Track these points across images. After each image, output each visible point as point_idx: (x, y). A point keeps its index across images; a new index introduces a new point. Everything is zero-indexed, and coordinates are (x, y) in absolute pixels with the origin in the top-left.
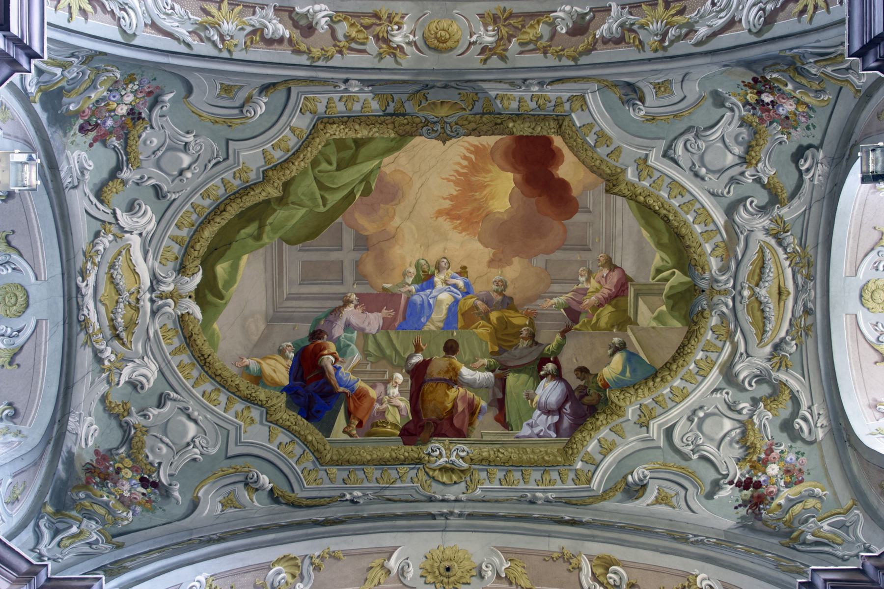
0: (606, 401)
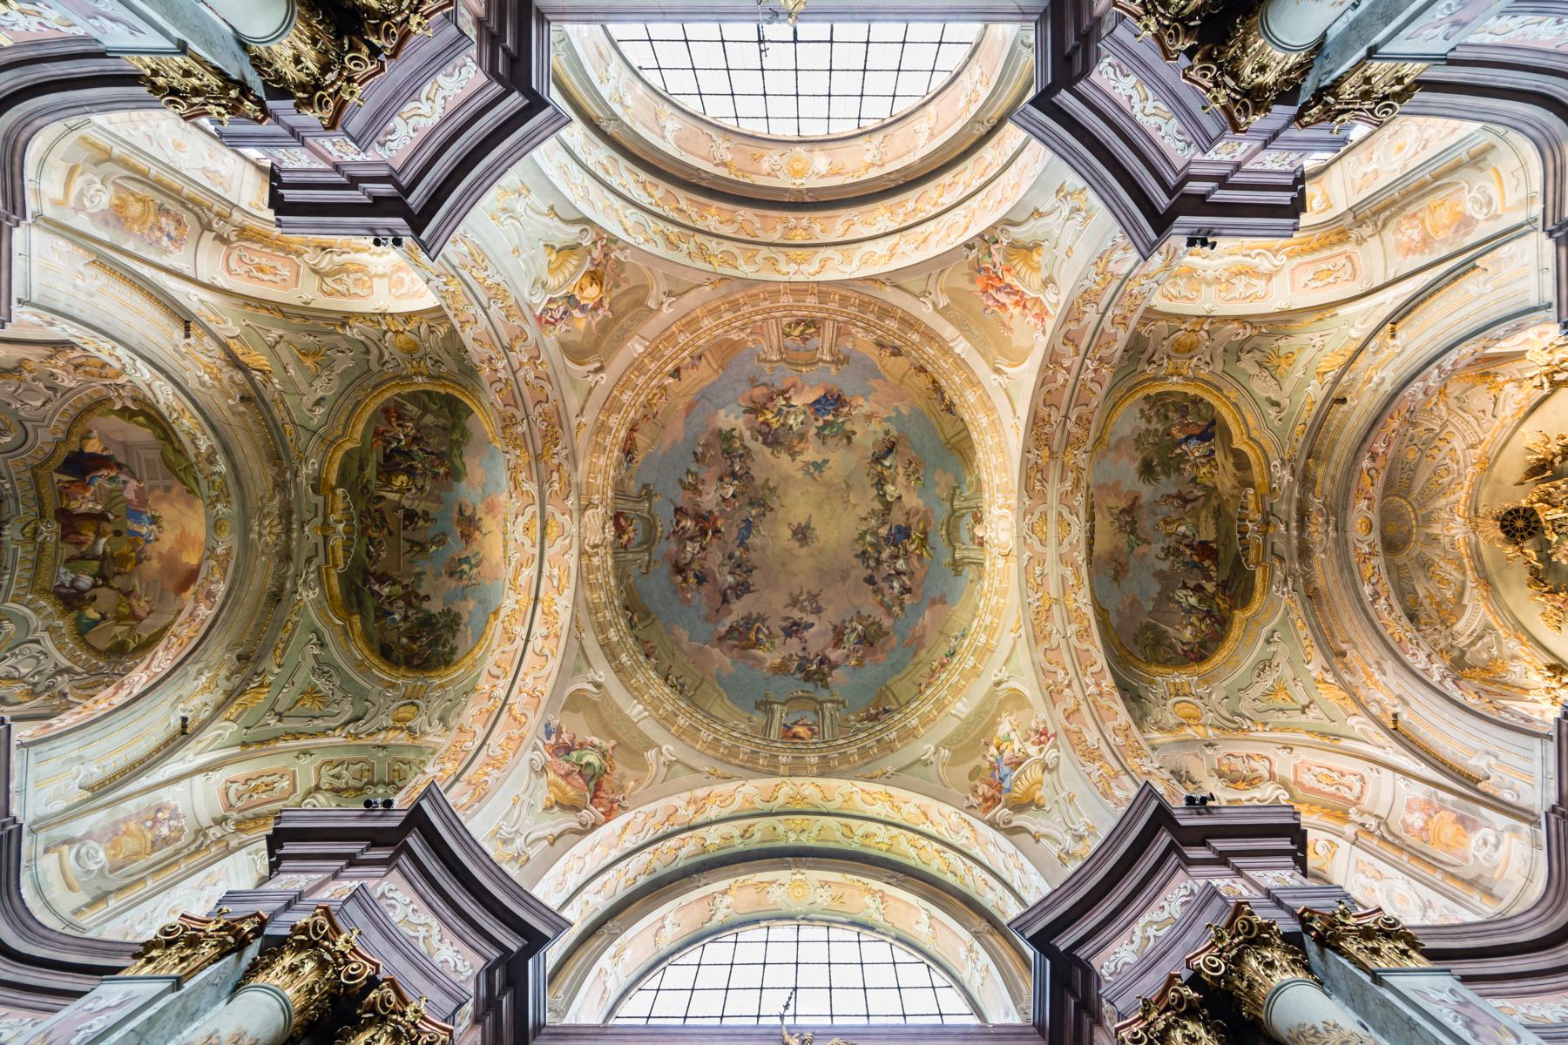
0: (71, 610)
